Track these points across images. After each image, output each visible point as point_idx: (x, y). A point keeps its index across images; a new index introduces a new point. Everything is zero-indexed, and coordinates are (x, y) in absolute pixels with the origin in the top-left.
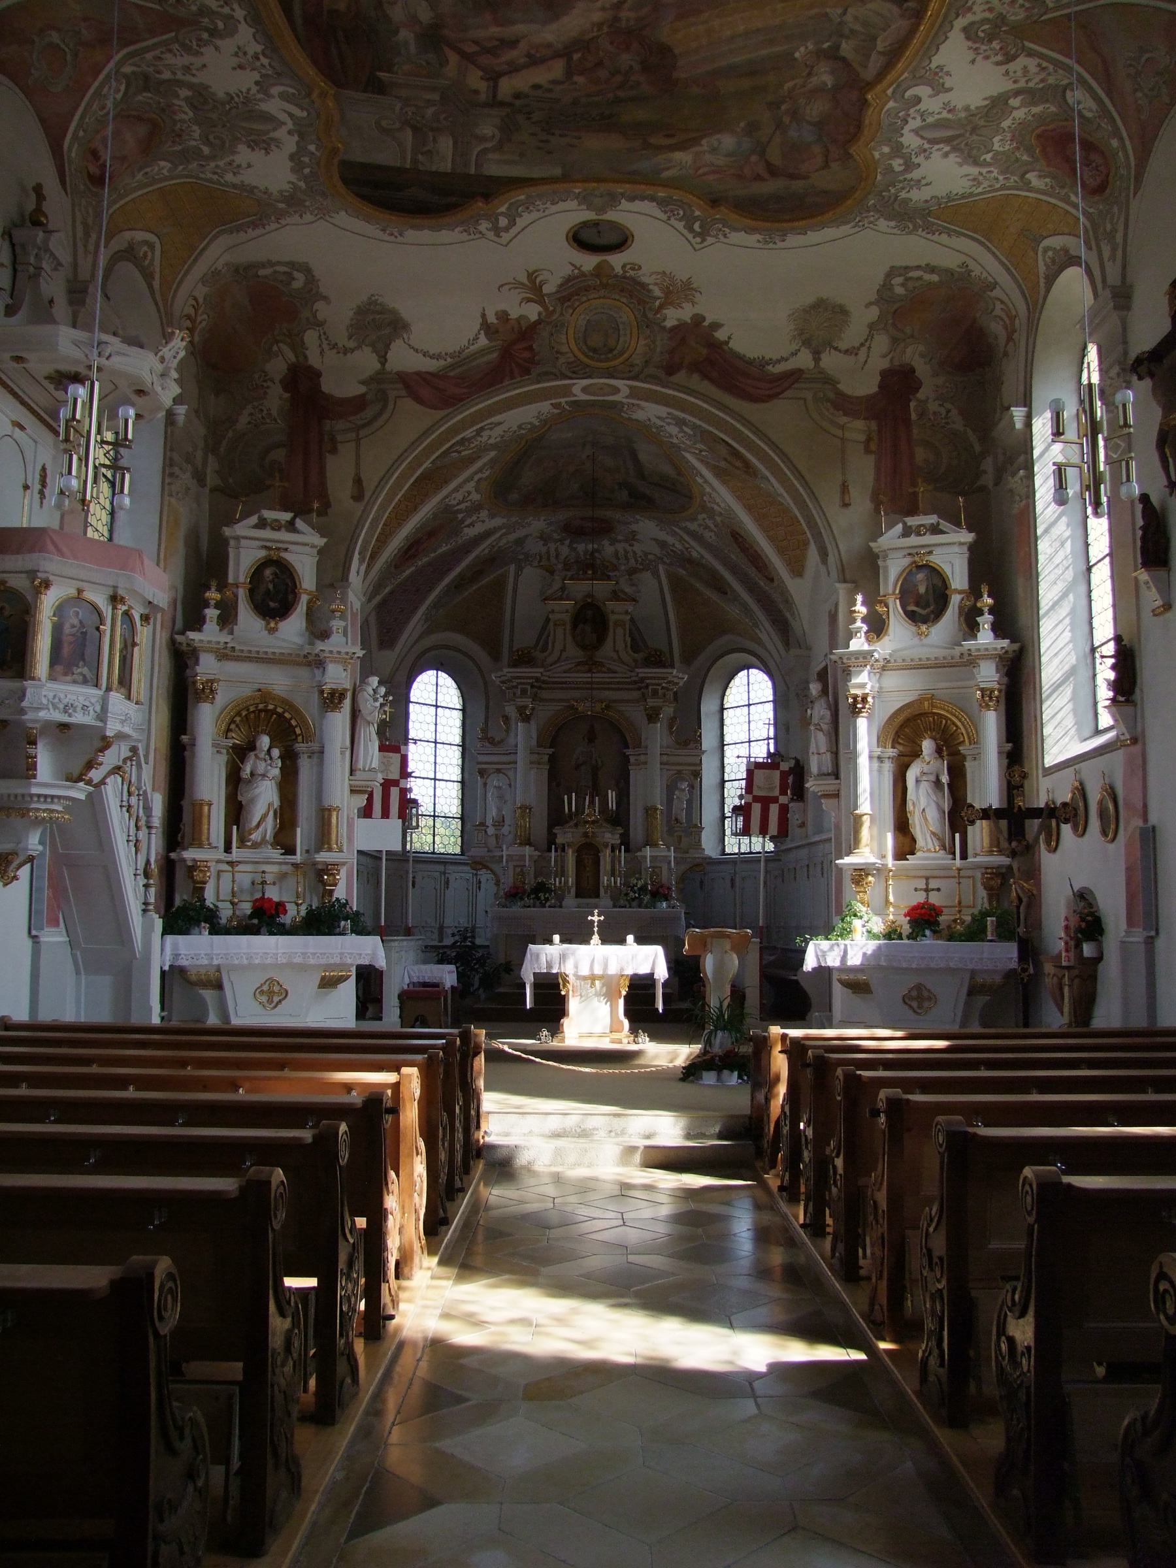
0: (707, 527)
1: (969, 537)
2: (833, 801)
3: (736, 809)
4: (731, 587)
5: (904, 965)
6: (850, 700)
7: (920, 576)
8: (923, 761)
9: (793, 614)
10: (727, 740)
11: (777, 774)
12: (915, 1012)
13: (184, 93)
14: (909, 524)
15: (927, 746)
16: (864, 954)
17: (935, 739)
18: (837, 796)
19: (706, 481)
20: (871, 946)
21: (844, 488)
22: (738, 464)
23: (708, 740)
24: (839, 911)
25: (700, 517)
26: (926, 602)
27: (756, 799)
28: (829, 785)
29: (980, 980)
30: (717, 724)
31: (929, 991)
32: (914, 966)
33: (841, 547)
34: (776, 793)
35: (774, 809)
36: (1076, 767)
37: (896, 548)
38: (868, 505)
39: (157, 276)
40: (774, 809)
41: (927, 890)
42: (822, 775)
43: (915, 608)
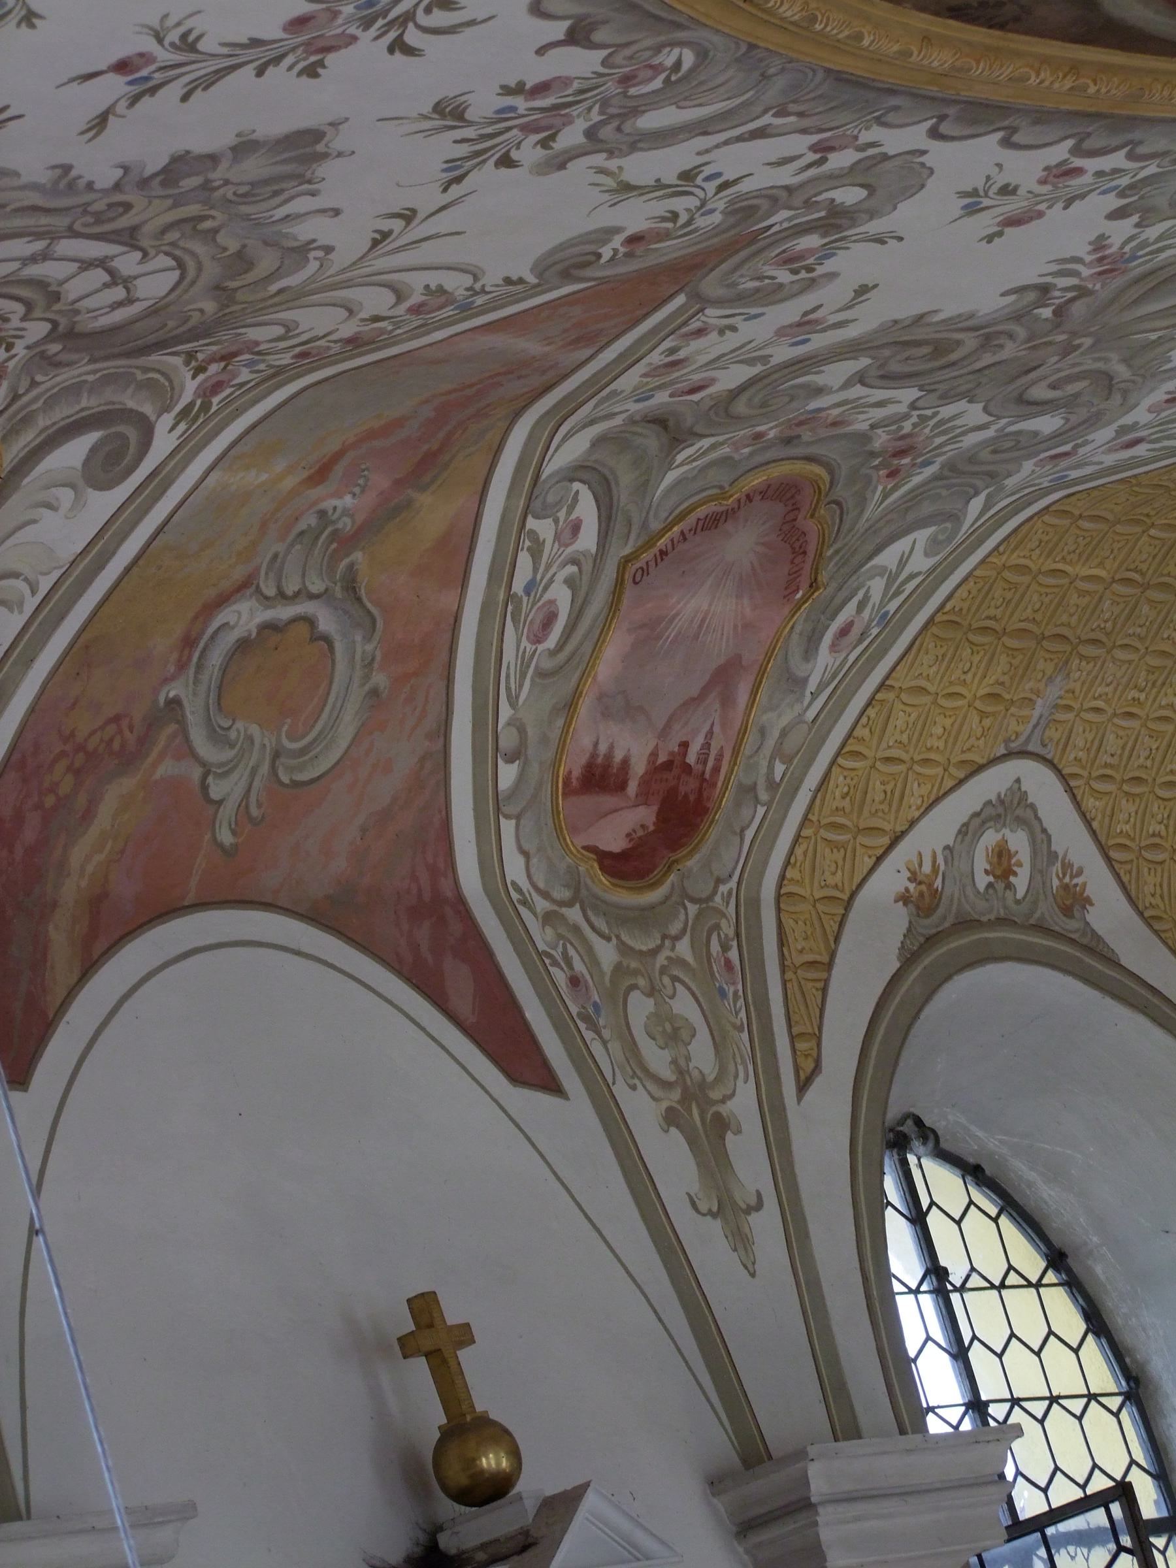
13: (835, 374)
39: (1099, 882)
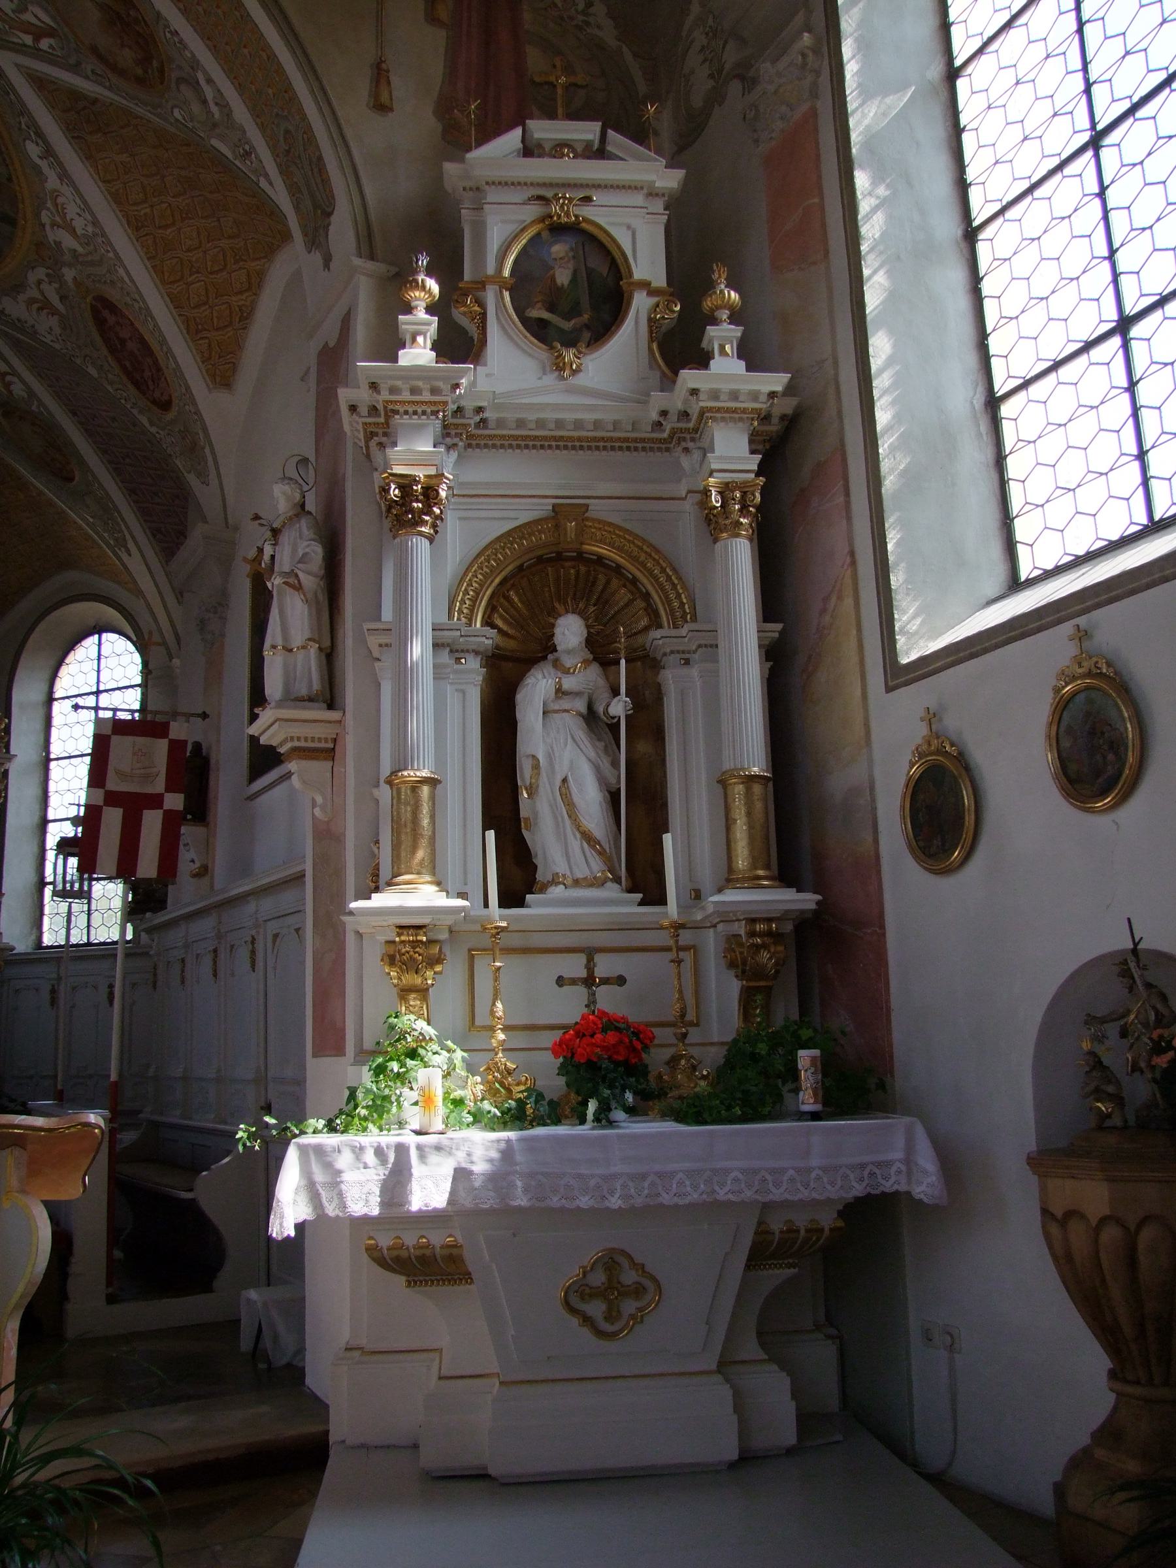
0: (45, 305)
1: (670, 179)
2: (319, 767)
3: (66, 846)
4: (82, 463)
5: (584, 1202)
6: (394, 492)
7: (559, 249)
8: (557, 664)
9: (202, 476)
10: (56, 750)
11: (162, 746)
12: (600, 1333)
14: (537, 135)
15: (570, 631)
16: (461, 1175)
17: (582, 614)
18: (329, 752)
19: (49, 152)
20: (480, 1147)
21: (380, 74)
22: (127, 57)
23: (22, 745)
24: (331, 1041)
25: (32, 277)
26: (575, 300)
27: (113, 799)
28: (312, 724)
29: (776, 1226)
30: (39, 725)
31: (641, 1268)
32: (615, 1202)
33: (368, 191)
34: (159, 786)
35: (152, 823)
36: (1082, 621)
37: (506, 185)
38: (429, 123)
40: (152, 823)
41: (589, 981)
42: (291, 699)
43: (546, 315)
